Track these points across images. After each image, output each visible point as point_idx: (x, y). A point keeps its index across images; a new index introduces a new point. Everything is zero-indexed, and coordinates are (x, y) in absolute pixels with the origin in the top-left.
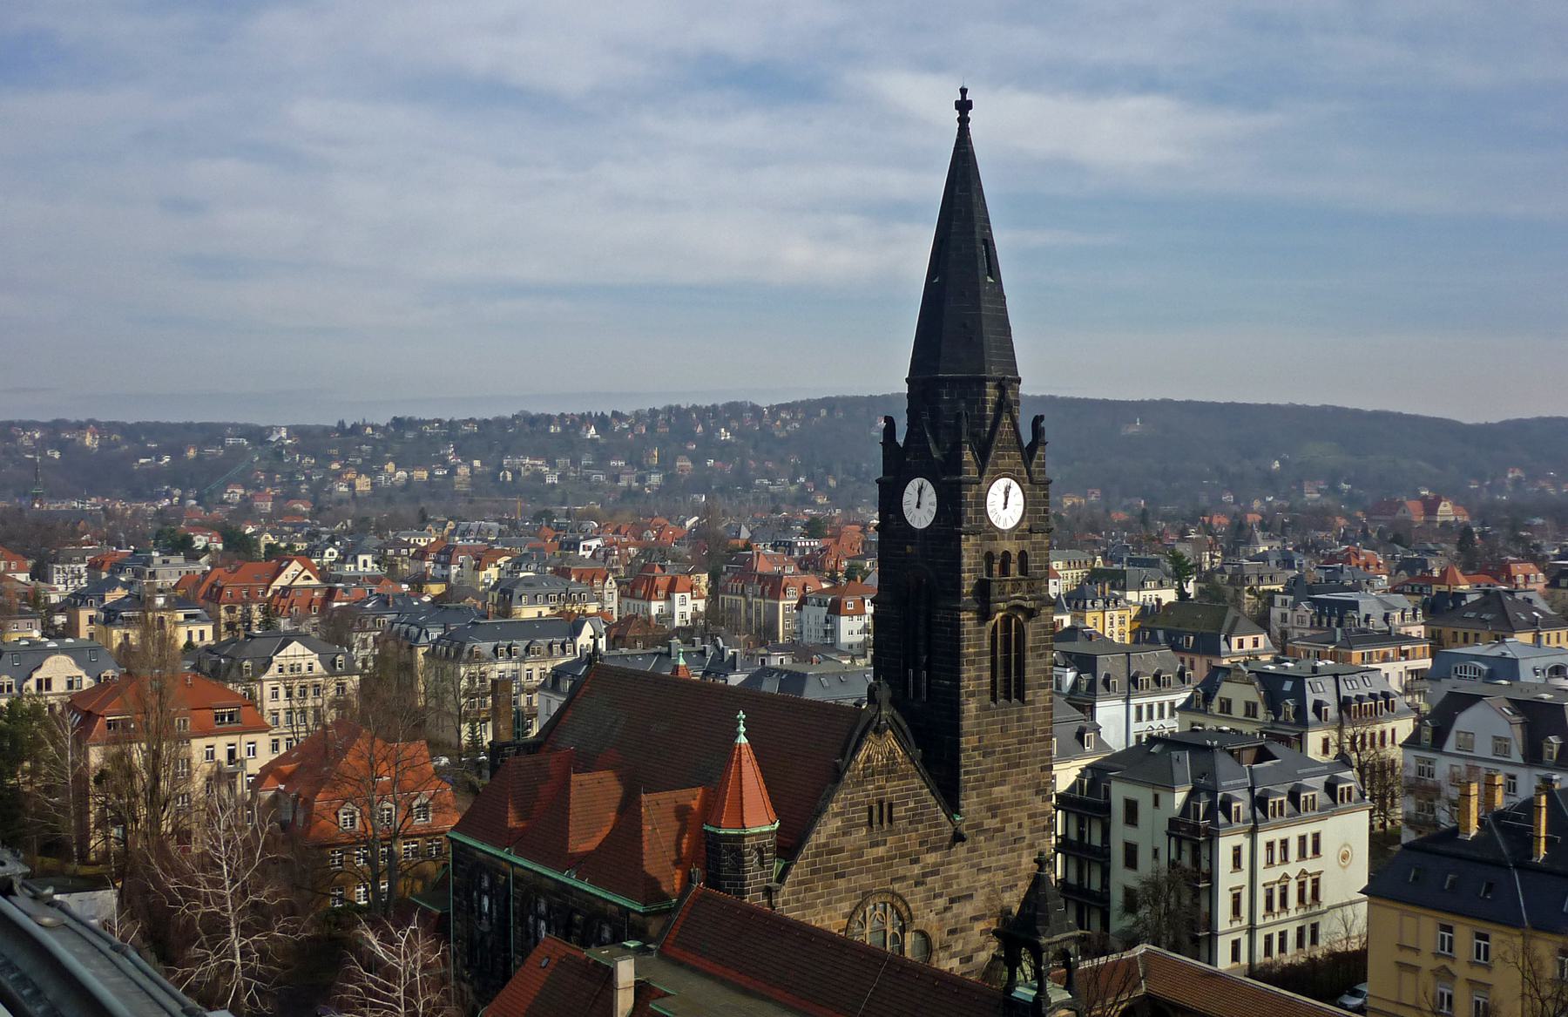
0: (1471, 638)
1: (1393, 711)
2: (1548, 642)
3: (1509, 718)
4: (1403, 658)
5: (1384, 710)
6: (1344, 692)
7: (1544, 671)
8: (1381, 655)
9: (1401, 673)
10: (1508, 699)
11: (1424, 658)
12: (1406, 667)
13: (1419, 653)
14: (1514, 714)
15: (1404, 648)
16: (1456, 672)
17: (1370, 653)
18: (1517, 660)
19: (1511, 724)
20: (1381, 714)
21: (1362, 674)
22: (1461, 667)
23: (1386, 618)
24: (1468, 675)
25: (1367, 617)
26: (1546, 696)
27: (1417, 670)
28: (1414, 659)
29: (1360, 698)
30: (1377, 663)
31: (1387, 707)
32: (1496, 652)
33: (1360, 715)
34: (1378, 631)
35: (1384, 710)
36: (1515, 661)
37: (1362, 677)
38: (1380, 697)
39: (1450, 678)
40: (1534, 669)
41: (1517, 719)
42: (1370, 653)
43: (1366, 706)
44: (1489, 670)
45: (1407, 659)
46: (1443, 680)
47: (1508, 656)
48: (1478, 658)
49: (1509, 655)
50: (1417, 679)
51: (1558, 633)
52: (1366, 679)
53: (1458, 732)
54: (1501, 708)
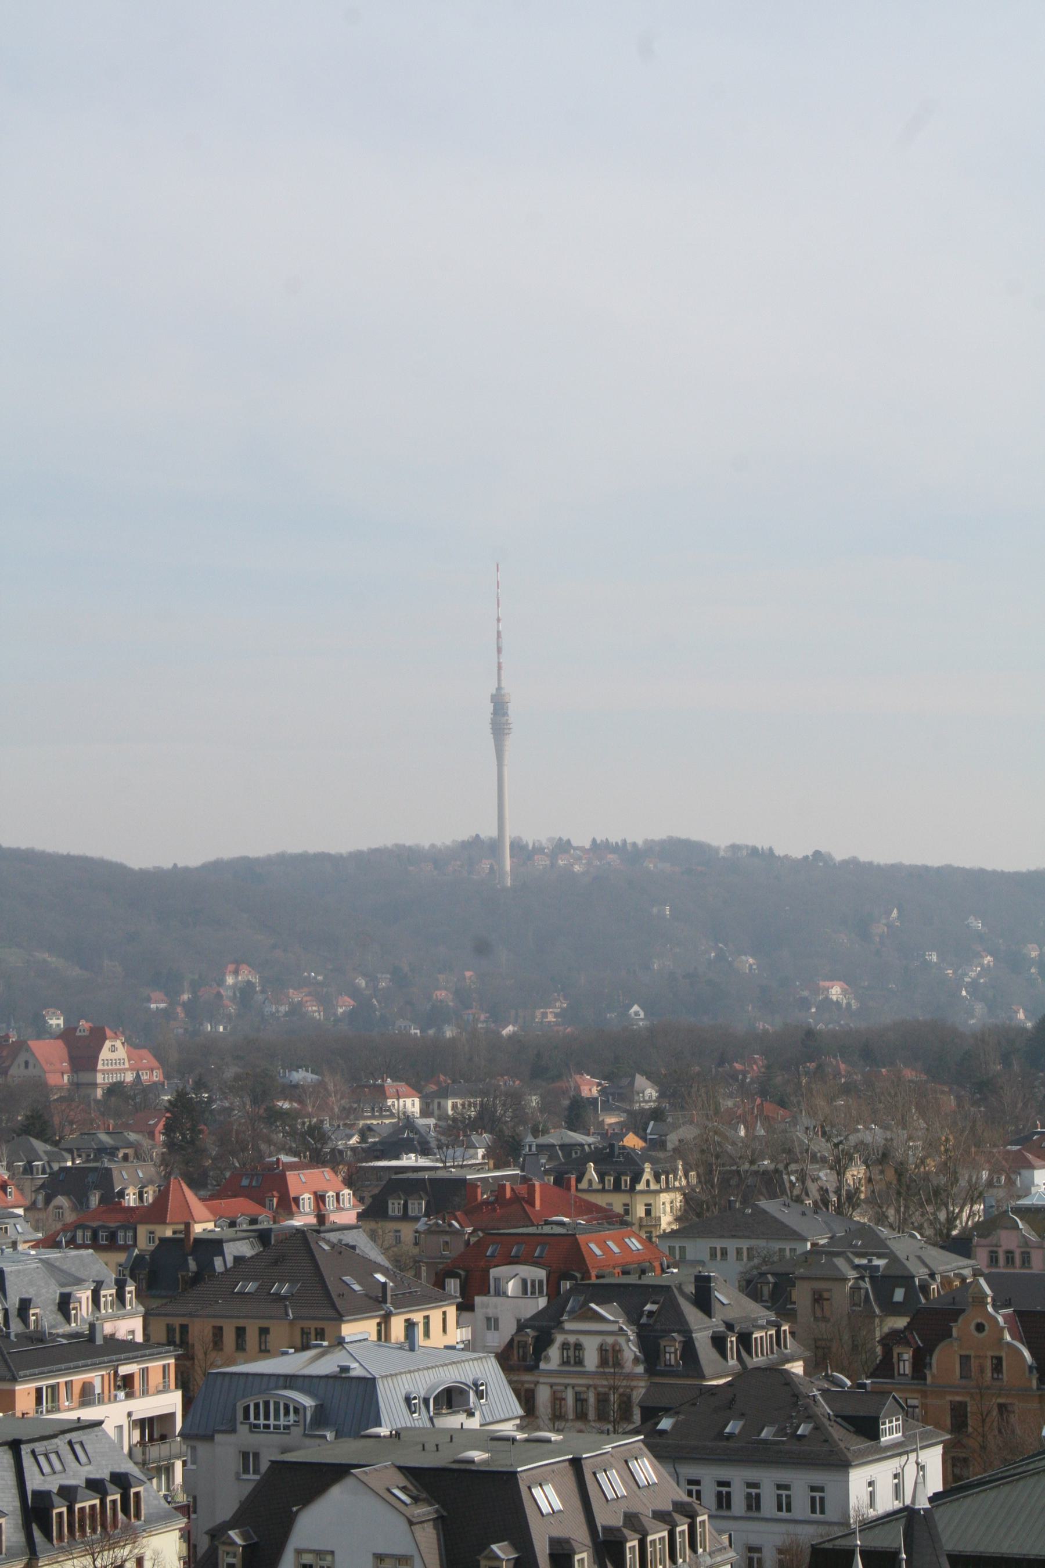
0: (252, 1337)
1: (138, 1516)
2: (427, 1334)
3: (408, 1511)
4: (122, 1395)
5: (120, 1515)
6: (35, 1482)
7: (426, 1401)
8: (77, 1389)
9: (120, 1427)
10: (400, 1468)
11: (165, 1389)
12: (130, 1414)
13: (155, 1378)
14: (416, 1500)
15: (124, 1370)
16: (247, 1416)
17: (54, 1388)
18: (374, 1379)
19: (411, 1523)
20: (115, 1525)
21: (68, 1436)
22: (257, 1405)
23: (64, 1305)
24: (272, 1422)
25: (25, 1305)
26: (478, 1456)
27: (151, 1420)
28: (145, 1393)
29: (68, 1493)
30: (70, 1409)
31: (125, 1510)
32: (327, 1366)
33: (104, 1526)
34: (64, 1336)
35: (120, 1515)
36: (369, 1384)
37: (70, 1443)
38: (110, 1487)
39: (233, 1431)
40: (408, 1400)
41: (424, 1511)
42: (54, 1388)
43: (82, 1509)
44: (316, 1406)
45: (130, 1395)
46: (218, 1437)
47: (353, 1374)
48: (290, 1381)
49: (357, 1371)
50: (151, 1439)
51: (444, 1313)
52: (78, 1448)
53: (299, 1552)
54: (389, 1490)
